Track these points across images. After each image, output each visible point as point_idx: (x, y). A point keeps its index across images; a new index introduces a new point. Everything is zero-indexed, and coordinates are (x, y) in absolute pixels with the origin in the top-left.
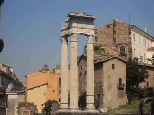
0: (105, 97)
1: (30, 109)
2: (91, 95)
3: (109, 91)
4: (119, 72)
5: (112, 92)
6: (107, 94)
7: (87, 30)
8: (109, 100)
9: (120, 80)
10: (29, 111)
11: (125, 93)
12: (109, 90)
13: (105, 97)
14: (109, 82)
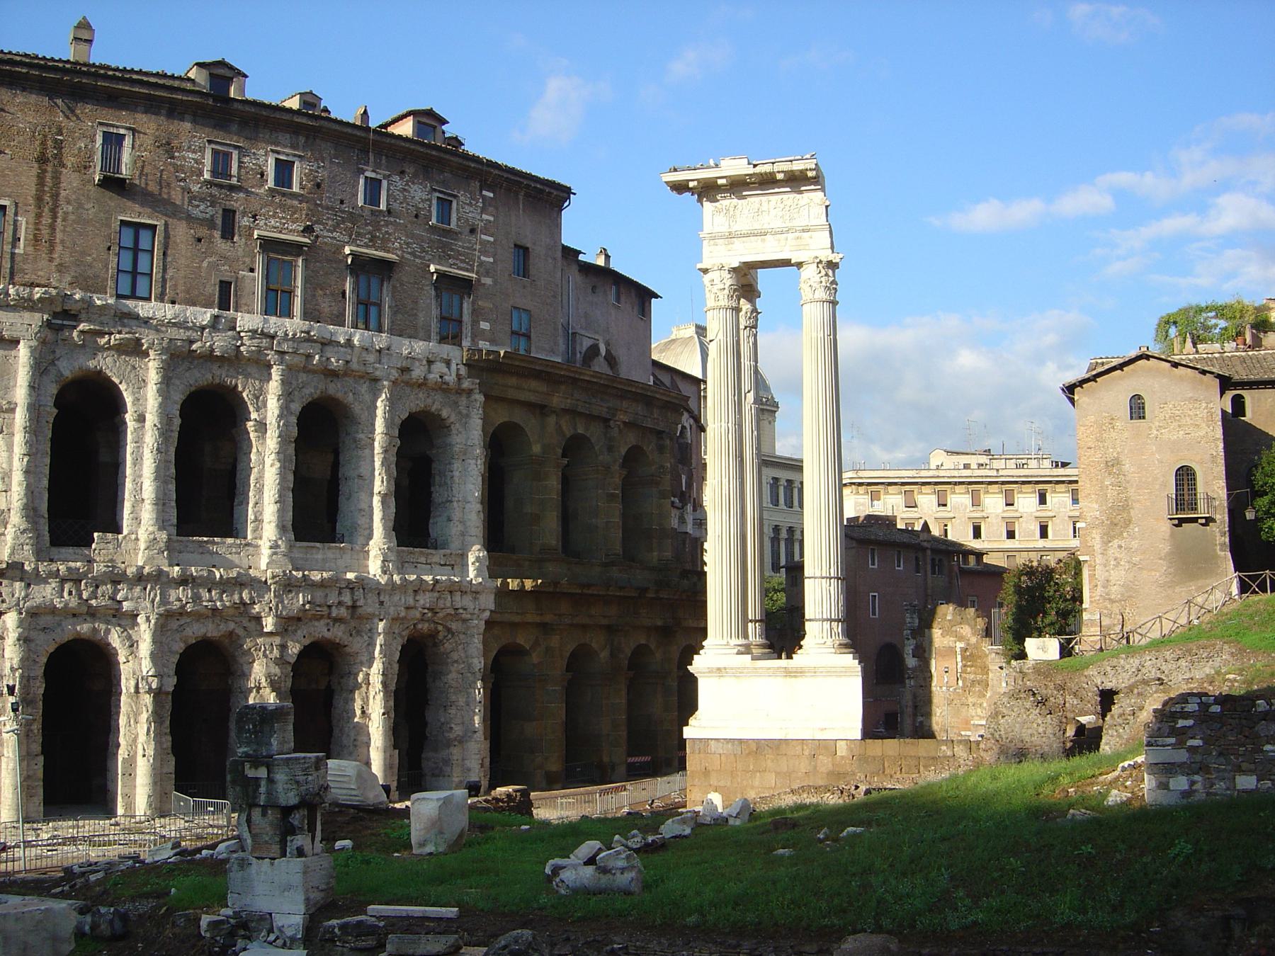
0: (1092, 576)
1: (961, 638)
2: (818, 574)
3: (1116, 543)
4: (1173, 434)
5: (1135, 544)
6: (1099, 559)
7: (790, 236)
8: (1115, 591)
9: (1185, 476)
10: (960, 645)
11: (1223, 545)
12: (1113, 537)
13: (1092, 576)
14: (1111, 493)
